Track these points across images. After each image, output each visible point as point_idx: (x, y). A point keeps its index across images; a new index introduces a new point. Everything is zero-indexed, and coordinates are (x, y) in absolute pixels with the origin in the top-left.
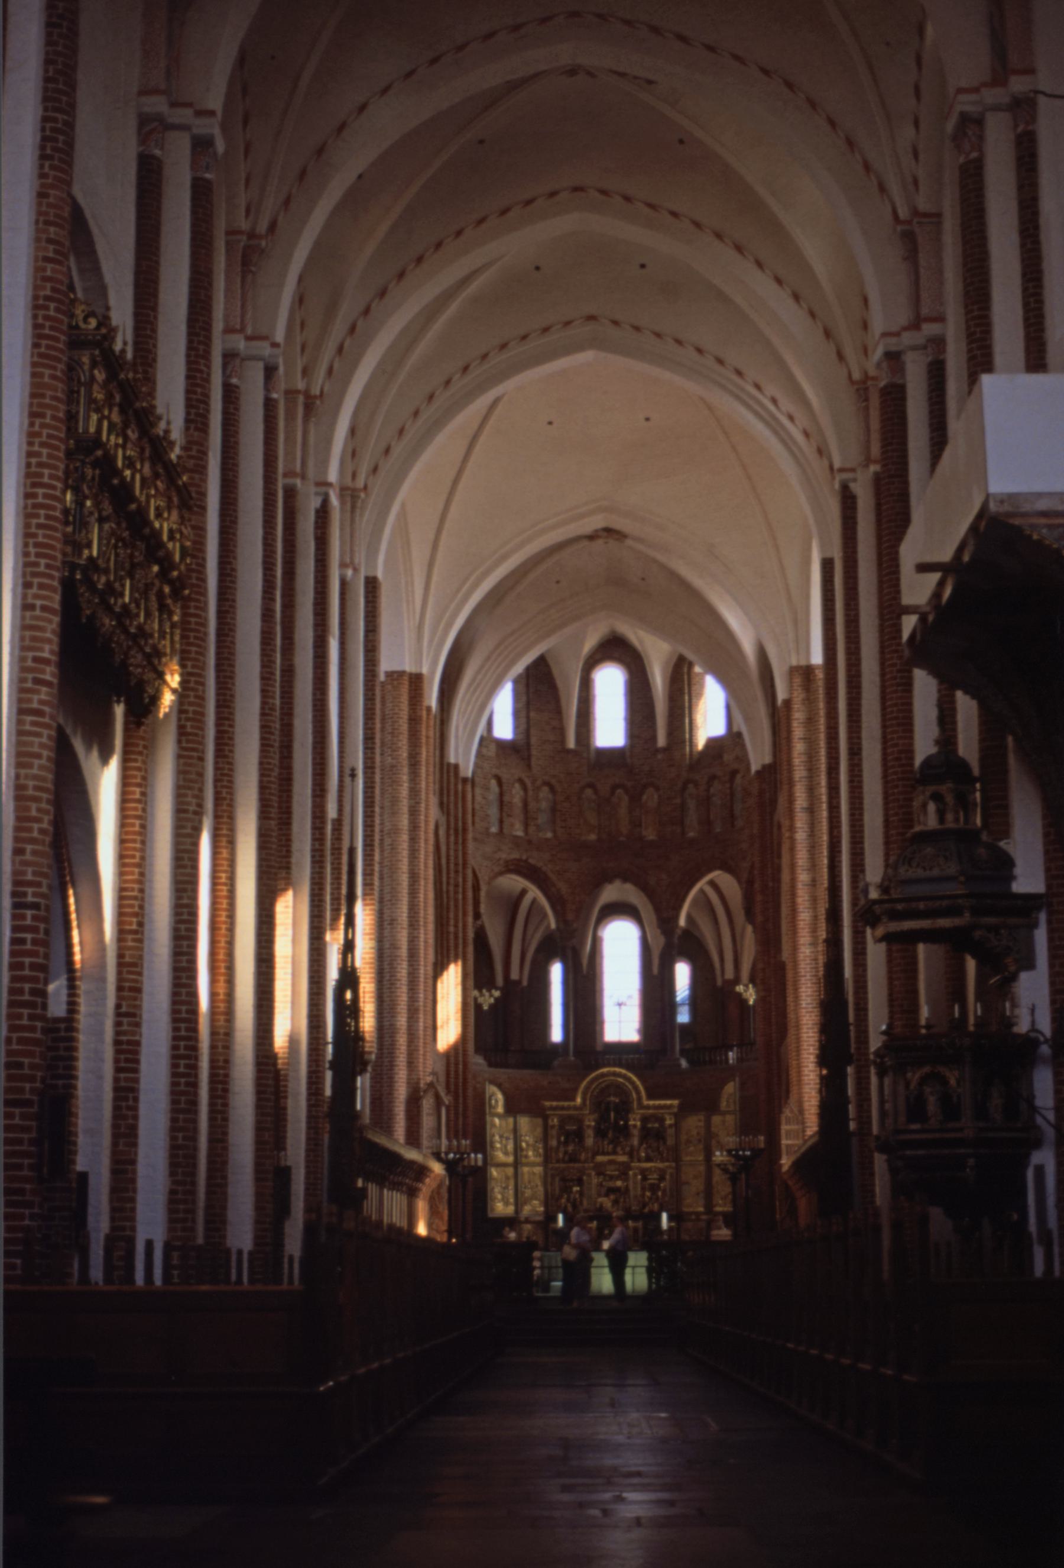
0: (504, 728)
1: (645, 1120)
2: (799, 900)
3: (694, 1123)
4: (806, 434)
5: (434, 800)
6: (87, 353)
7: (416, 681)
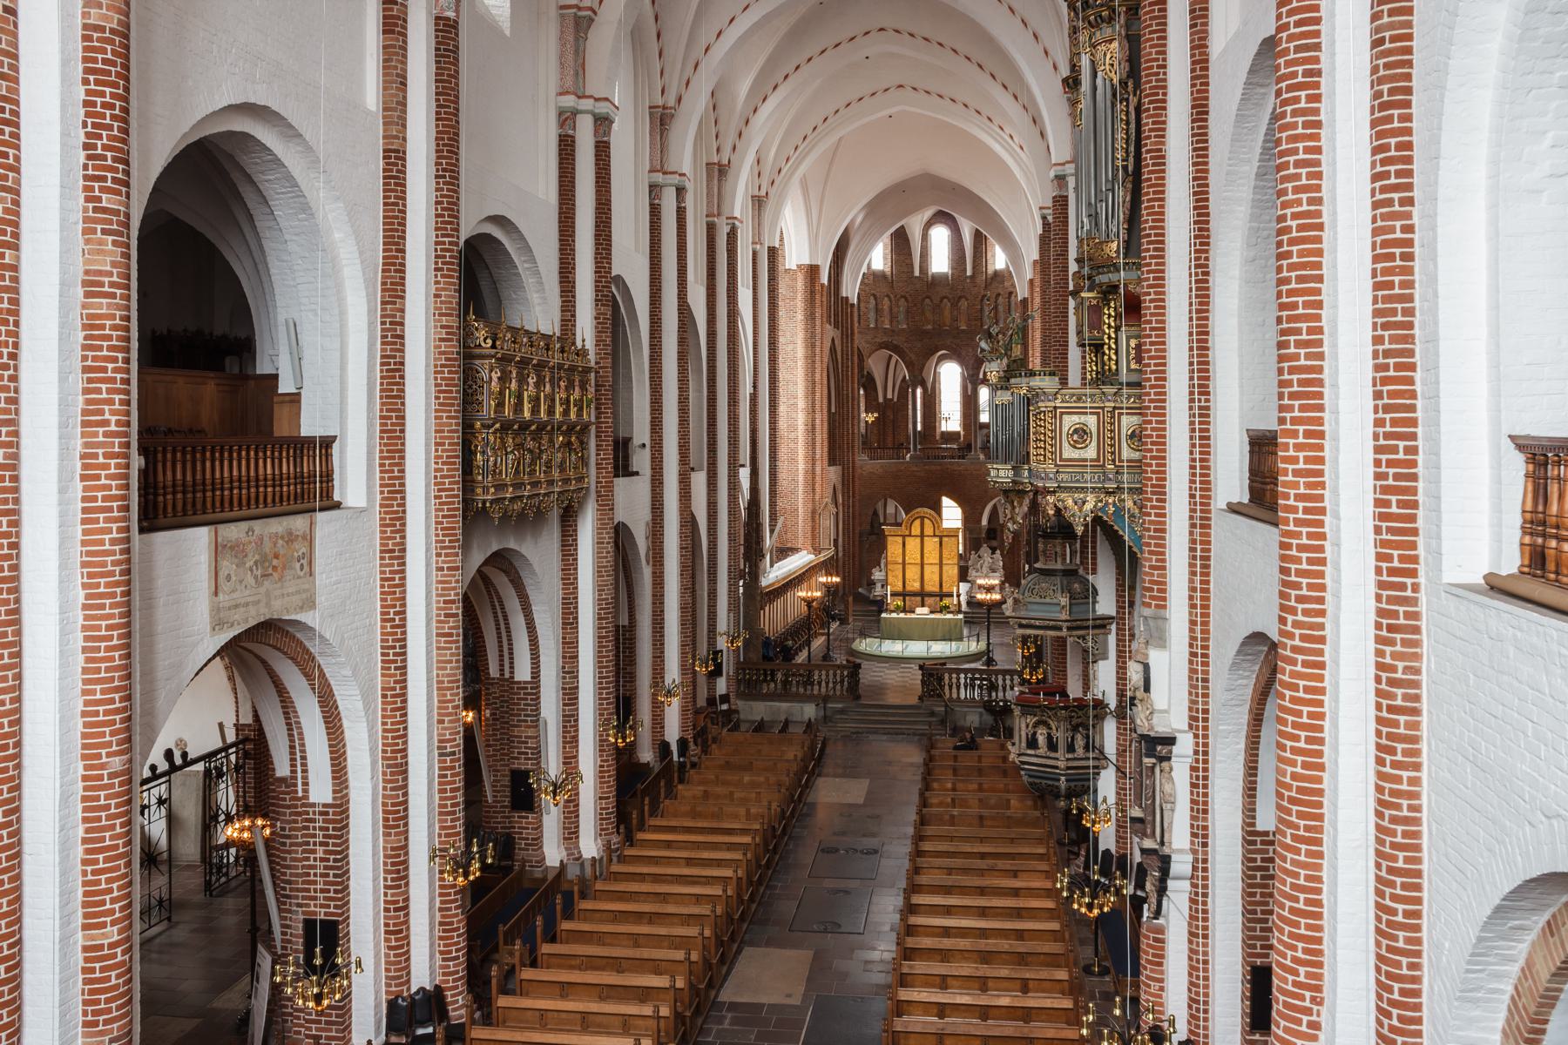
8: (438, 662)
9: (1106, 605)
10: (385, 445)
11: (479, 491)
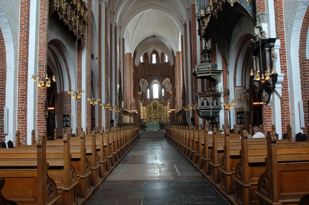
0: (142, 61)
3: (165, 107)
7: (130, 54)
8: (40, 37)
9: (220, 68)
11: (55, 5)
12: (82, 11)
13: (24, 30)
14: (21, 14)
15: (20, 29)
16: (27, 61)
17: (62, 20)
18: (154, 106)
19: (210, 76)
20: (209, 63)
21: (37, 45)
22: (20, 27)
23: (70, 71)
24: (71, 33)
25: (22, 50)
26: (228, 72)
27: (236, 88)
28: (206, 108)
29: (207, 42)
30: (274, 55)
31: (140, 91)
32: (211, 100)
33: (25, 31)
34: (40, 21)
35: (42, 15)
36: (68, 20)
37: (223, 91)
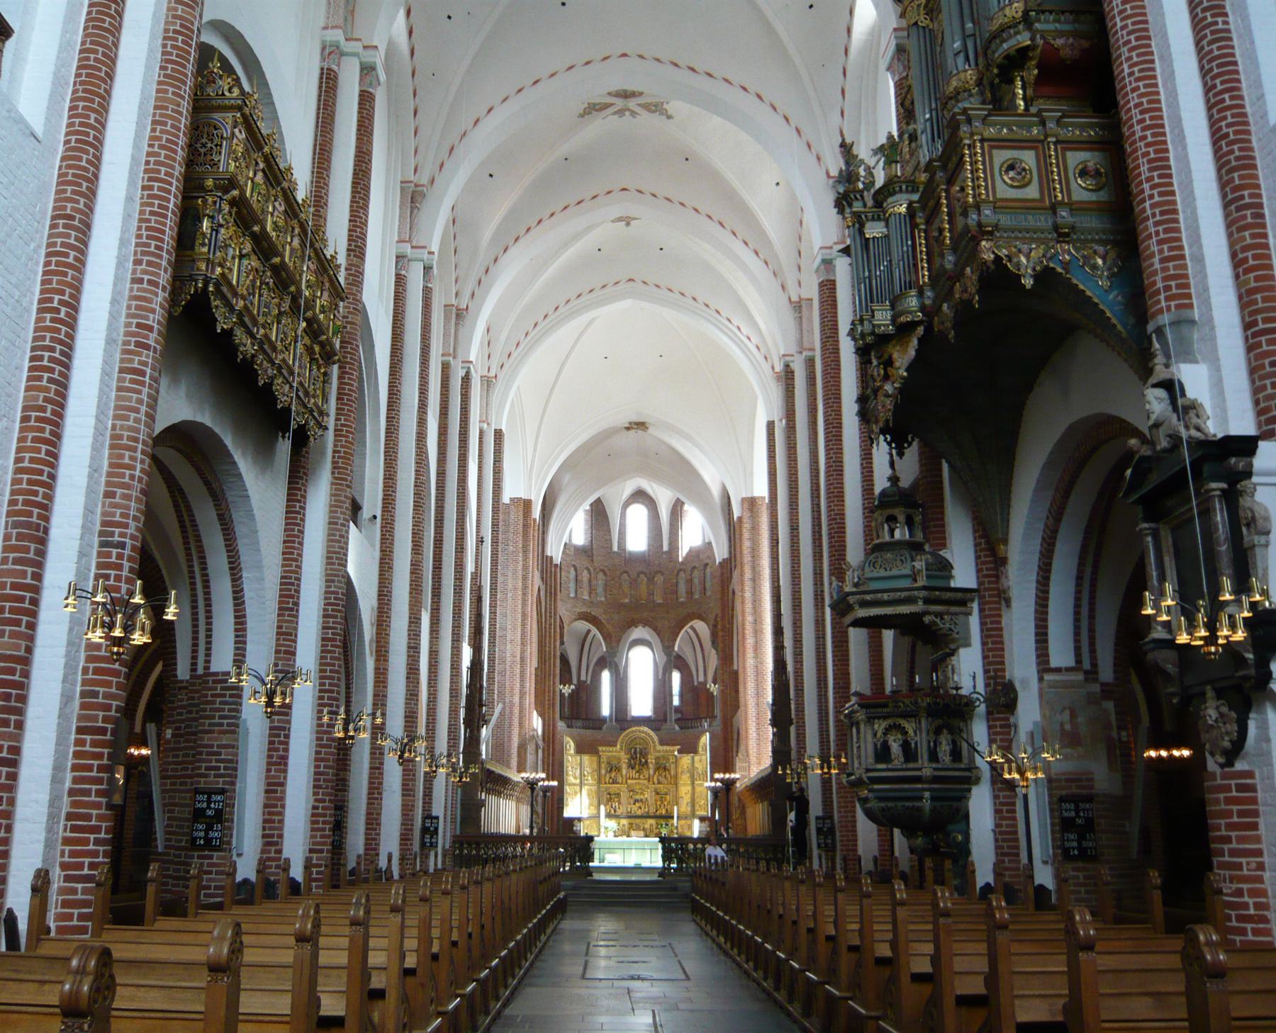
1: (657, 758)
2: (747, 632)
3: (686, 760)
4: (758, 348)
5: (537, 574)
6: (230, 115)
7: (527, 504)
8: (117, 408)
9: (964, 575)
10: (82, 83)
12: (323, 300)
13: (46, 375)
14: (41, 301)
15: (31, 369)
16: (47, 519)
17: (228, 334)
18: (635, 753)
19: (917, 617)
20: (913, 553)
21: (103, 445)
22: (32, 359)
23: (244, 575)
24: (267, 394)
25: (26, 464)
26: (1003, 598)
27: (1047, 677)
28: (901, 774)
29: (901, 454)
30: (1253, 518)
31: (565, 679)
32: (924, 735)
33: (50, 380)
34: (127, 334)
35: (138, 307)
36: (252, 336)
37: (983, 693)
